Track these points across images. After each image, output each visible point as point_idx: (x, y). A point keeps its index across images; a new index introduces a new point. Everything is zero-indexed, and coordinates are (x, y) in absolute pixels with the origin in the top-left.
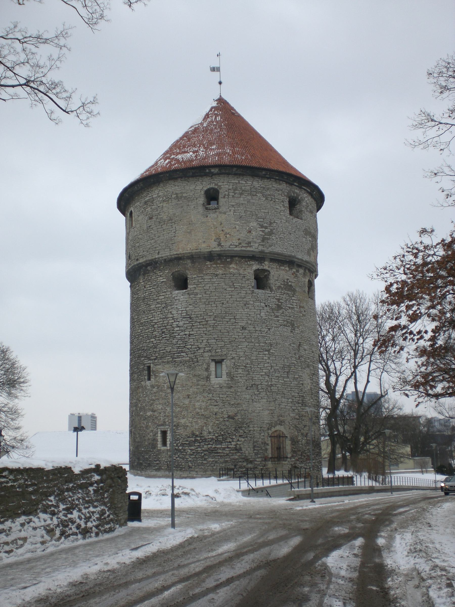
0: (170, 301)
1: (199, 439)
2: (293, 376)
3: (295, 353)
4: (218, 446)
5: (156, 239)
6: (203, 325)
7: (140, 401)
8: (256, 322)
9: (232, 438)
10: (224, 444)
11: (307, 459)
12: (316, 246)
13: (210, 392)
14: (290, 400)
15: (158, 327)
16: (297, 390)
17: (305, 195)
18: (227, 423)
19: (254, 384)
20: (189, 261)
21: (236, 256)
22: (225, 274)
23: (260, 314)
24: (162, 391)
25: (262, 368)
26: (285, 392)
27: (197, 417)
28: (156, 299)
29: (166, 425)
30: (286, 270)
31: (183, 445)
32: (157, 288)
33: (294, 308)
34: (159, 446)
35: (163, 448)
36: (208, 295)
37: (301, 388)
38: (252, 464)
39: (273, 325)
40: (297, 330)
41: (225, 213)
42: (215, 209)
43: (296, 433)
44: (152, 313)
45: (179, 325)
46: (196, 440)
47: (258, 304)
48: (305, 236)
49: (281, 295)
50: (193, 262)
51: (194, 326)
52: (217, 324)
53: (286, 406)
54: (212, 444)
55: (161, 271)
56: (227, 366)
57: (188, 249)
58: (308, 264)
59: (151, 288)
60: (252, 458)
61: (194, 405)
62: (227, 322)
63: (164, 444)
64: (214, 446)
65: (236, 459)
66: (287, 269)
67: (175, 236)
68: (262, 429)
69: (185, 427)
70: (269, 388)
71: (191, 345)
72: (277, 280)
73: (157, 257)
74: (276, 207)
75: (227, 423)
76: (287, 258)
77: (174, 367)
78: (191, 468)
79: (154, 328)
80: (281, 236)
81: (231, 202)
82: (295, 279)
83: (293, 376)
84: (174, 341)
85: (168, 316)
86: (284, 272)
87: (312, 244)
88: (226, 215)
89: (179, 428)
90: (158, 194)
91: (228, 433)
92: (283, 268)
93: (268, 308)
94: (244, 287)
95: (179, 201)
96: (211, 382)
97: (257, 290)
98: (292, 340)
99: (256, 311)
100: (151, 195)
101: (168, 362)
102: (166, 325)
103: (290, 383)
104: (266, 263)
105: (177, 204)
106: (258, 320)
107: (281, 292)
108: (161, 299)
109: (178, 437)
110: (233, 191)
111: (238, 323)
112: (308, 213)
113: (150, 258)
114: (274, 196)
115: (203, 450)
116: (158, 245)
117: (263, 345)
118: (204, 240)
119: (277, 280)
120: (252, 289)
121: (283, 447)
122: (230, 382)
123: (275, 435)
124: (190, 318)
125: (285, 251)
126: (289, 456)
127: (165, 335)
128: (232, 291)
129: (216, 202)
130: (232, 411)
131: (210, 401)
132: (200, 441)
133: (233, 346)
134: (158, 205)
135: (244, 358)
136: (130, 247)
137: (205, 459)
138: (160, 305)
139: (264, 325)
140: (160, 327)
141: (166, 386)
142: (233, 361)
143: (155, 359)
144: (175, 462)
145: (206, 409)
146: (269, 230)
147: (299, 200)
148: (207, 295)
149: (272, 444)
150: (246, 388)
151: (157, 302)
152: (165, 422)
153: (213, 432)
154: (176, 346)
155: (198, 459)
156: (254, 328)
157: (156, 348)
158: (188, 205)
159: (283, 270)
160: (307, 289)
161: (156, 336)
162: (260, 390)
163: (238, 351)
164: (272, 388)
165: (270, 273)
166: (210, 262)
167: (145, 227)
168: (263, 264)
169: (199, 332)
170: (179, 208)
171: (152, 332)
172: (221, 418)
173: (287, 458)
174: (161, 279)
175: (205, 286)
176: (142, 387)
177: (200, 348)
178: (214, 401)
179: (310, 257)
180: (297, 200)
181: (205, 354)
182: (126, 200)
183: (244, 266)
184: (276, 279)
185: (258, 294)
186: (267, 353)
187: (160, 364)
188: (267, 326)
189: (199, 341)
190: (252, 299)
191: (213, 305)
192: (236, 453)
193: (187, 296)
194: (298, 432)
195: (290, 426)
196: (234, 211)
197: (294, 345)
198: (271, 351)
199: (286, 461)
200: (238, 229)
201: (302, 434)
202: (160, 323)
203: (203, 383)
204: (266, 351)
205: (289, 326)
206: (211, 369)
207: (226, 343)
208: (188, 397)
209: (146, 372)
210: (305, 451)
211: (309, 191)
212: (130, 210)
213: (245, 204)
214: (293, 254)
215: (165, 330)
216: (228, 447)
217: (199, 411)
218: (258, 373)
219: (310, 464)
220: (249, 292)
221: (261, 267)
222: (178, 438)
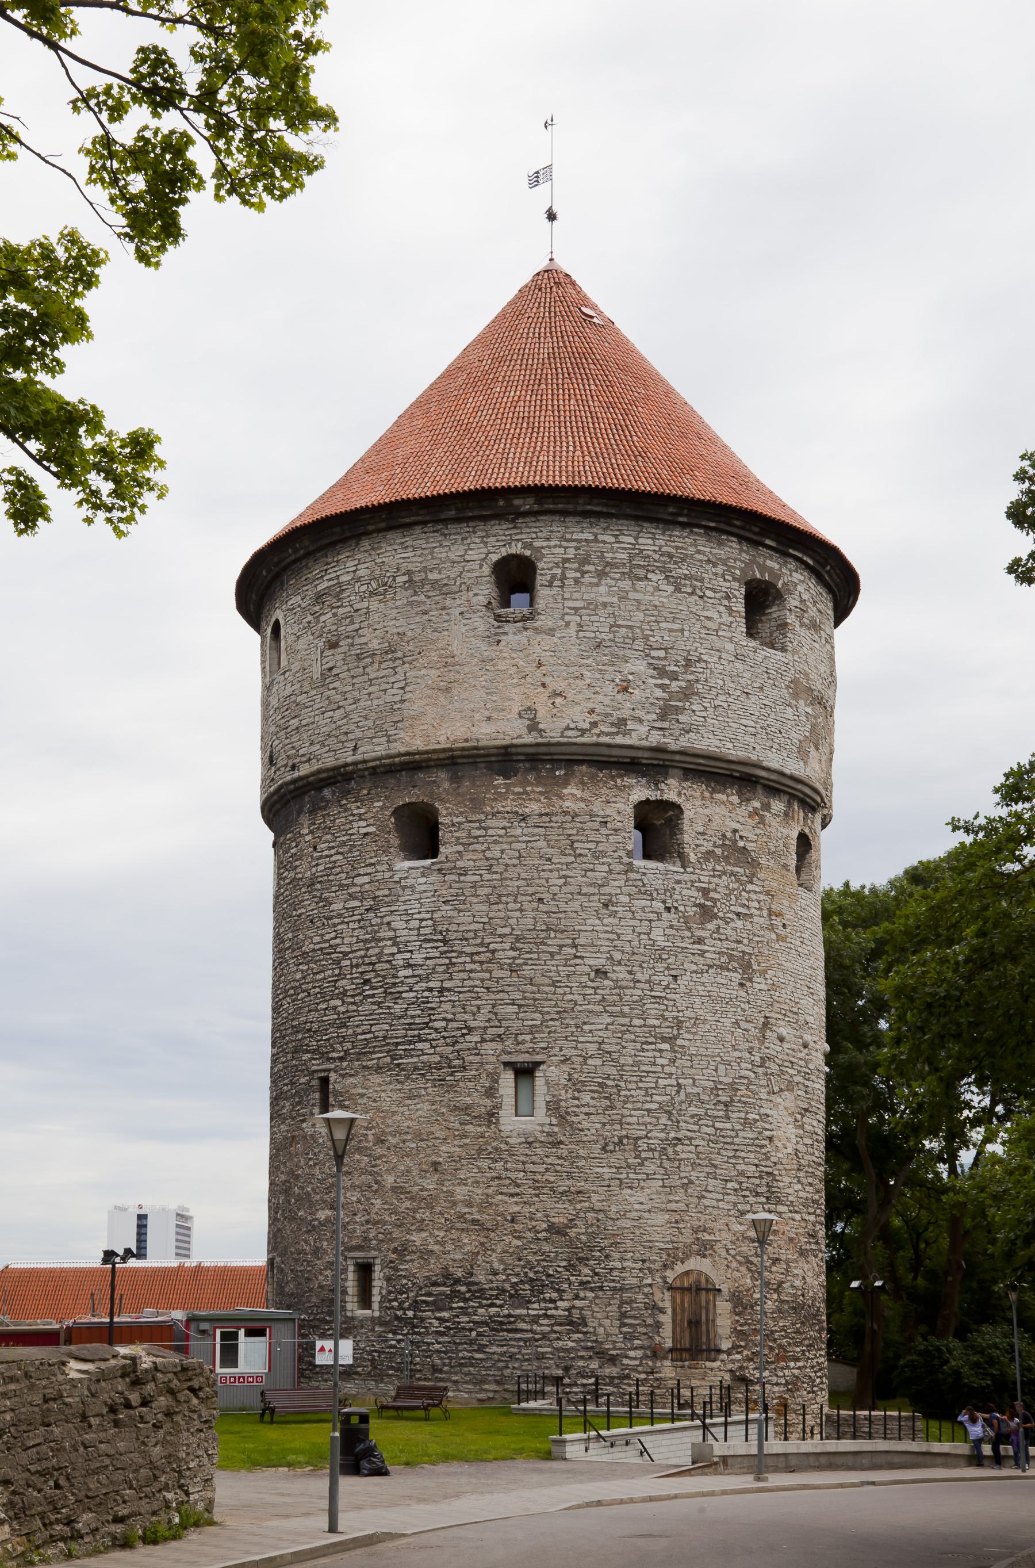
0: (387, 892)
1: (463, 1289)
2: (742, 1115)
3: (752, 1048)
4: (518, 1312)
5: (349, 708)
6: (481, 963)
7: (297, 1177)
8: (635, 957)
9: (558, 1291)
10: (536, 1306)
11: (778, 1358)
12: (830, 730)
13: (496, 1155)
14: (730, 1185)
16: (752, 1156)
17: (797, 576)
18: (546, 1247)
19: (626, 1137)
20: (443, 775)
21: (581, 762)
22: (547, 814)
23: (648, 934)
25: (650, 1091)
26: (718, 1160)
27: (459, 1225)
28: (348, 886)
29: (370, 1249)
30: (732, 804)
31: (416, 1305)
32: (350, 851)
33: (752, 915)
34: (349, 1306)
35: (361, 1313)
36: (497, 877)
37: (764, 1150)
38: (615, 1365)
39: (687, 966)
40: (759, 983)
41: (551, 632)
42: (524, 619)
43: (749, 1281)
44: (335, 925)
45: (411, 962)
46: (455, 1294)
47: (643, 903)
48: (793, 702)
49: (714, 876)
50: (455, 779)
51: (454, 964)
52: (521, 961)
53: (718, 1201)
54: (501, 1306)
55: (362, 801)
56: (547, 1083)
57: (442, 739)
59: (333, 852)
60: (614, 1349)
61: (451, 1193)
62: (552, 954)
63: (365, 1301)
64: (506, 1312)
65: (567, 1350)
66: (735, 799)
67: (402, 701)
68: (647, 1265)
69: (426, 1254)
70: (670, 1150)
71: (444, 1019)
72: (704, 834)
73: (349, 760)
74: (706, 613)
75: (546, 1247)
76: (733, 767)
78: (441, 1371)
79: (341, 968)
80: (717, 703)
81: (568, 599)
82: (758, 831)
83: (742, 1115)
84: (397, 1009)
86: (725, 811)
87: (813, 725)
88: (556, 640)
89: (408, 1258)
90: (354, 571)
91: (549, 1276)
93: (672, 916)
94: (604, 854)
95: (416, 593)
96: (502, 1128)
97: (639, 863)
99: (637, 923)
100: (333, 575)
101: (378, 1069)
103: (733, 1134)
104: (670, 781)
105: (411, 604)
106: (642, 950)
107: (714, 870)
108: (361, 886)
109: (404, 1281)
110: (577, 565)
111: (582, 958)
112: (803, 631)
113: (329, 762)
114: (702, 581)
115: (475, 1323)
116: (353, 727)
117: (656, 1022)
118: (487, 713)
119: (704, 834)
120: (626, 860)
121: (707, 1320)
122: (556, 1129)
123: (686, 1285)
124: (445, 942)
125: (730, 746)
126: (725, 1345)
127: (372, 988)
128: (567, 864)
129: (527, 596)
130: (560, 1212)
131: (497, 1182)
132: (468, 1295)
133: (568, 1026)
134: (356, 607)
135: (599, 1062)
136: (273, 729)
137: (481, 1349)
138: (357, 903)
139: (660, 966)
140: (357, 966)
141: (371, 1138)
142: (566, 1068)
144: (395, 1354)
145: (486, 1204)
146: (683, 684)
147: (778, 591)
148: (495, 876)
149: (674, 1310)
150: (604, 1149)
151: (350, 895)
152: (366, 1239)
153: (505, 1270)
154: (402, 1021)
155: (460, 1347)
156: (630, 973)
157: (344, 1025)
158: (444, 608)
159: (723, 803)
160: (792, 860)
161: (346, 991)
162: (643, 1155)
163: (581, 1039)
164: (679, 1148)
165: (682, 812)
166: (507, 777)
168: (663, 786)
169: (471, 983)
170: (417, 613)
171: (336, 981)
172: (530, 1230)
173: (719, 1351)
174: (361, 827)
175: (489, 849)
176: (305, 1137)
177: (470, 1030)
178: (508, 1182)
179: (806, 763)
180: (773, 591)
181: (485, 1046)
182: (260, 587)
183: (604, 791)
184: (701, 830)
185: (644, 874)
186: (666, 1046)
188: (668, 968)
189: (468, 1008)
190: (625, 890)
191: (511, 906)
192: (569, 1332)
193: (434, 878)
194: (753, 1278)
195: (730, 1258)
196: (580, 625)
197: (749, 1026)
198: (679, 1042)
199: (714, 1361)
200: (588, 681)
201: (767, 1284)
202: (358, 954)
203: (479, 1129)
204: (664, 1039)
205: (734, 970)
206: (501, 1092)
207: (547, 1017)
208: (436, 1170)
209: (317, 1095)
210: (773, 1332)
211: (811, 562)
212: (273, 620)
213: (612, 604)
214: (754, 757)
216: (546, 1316)
217: (467, 1210)
218: (639, 1105)
219: (786, 1372)
220: (619, 868)
221: (653, 795)
222: (403, 1286)
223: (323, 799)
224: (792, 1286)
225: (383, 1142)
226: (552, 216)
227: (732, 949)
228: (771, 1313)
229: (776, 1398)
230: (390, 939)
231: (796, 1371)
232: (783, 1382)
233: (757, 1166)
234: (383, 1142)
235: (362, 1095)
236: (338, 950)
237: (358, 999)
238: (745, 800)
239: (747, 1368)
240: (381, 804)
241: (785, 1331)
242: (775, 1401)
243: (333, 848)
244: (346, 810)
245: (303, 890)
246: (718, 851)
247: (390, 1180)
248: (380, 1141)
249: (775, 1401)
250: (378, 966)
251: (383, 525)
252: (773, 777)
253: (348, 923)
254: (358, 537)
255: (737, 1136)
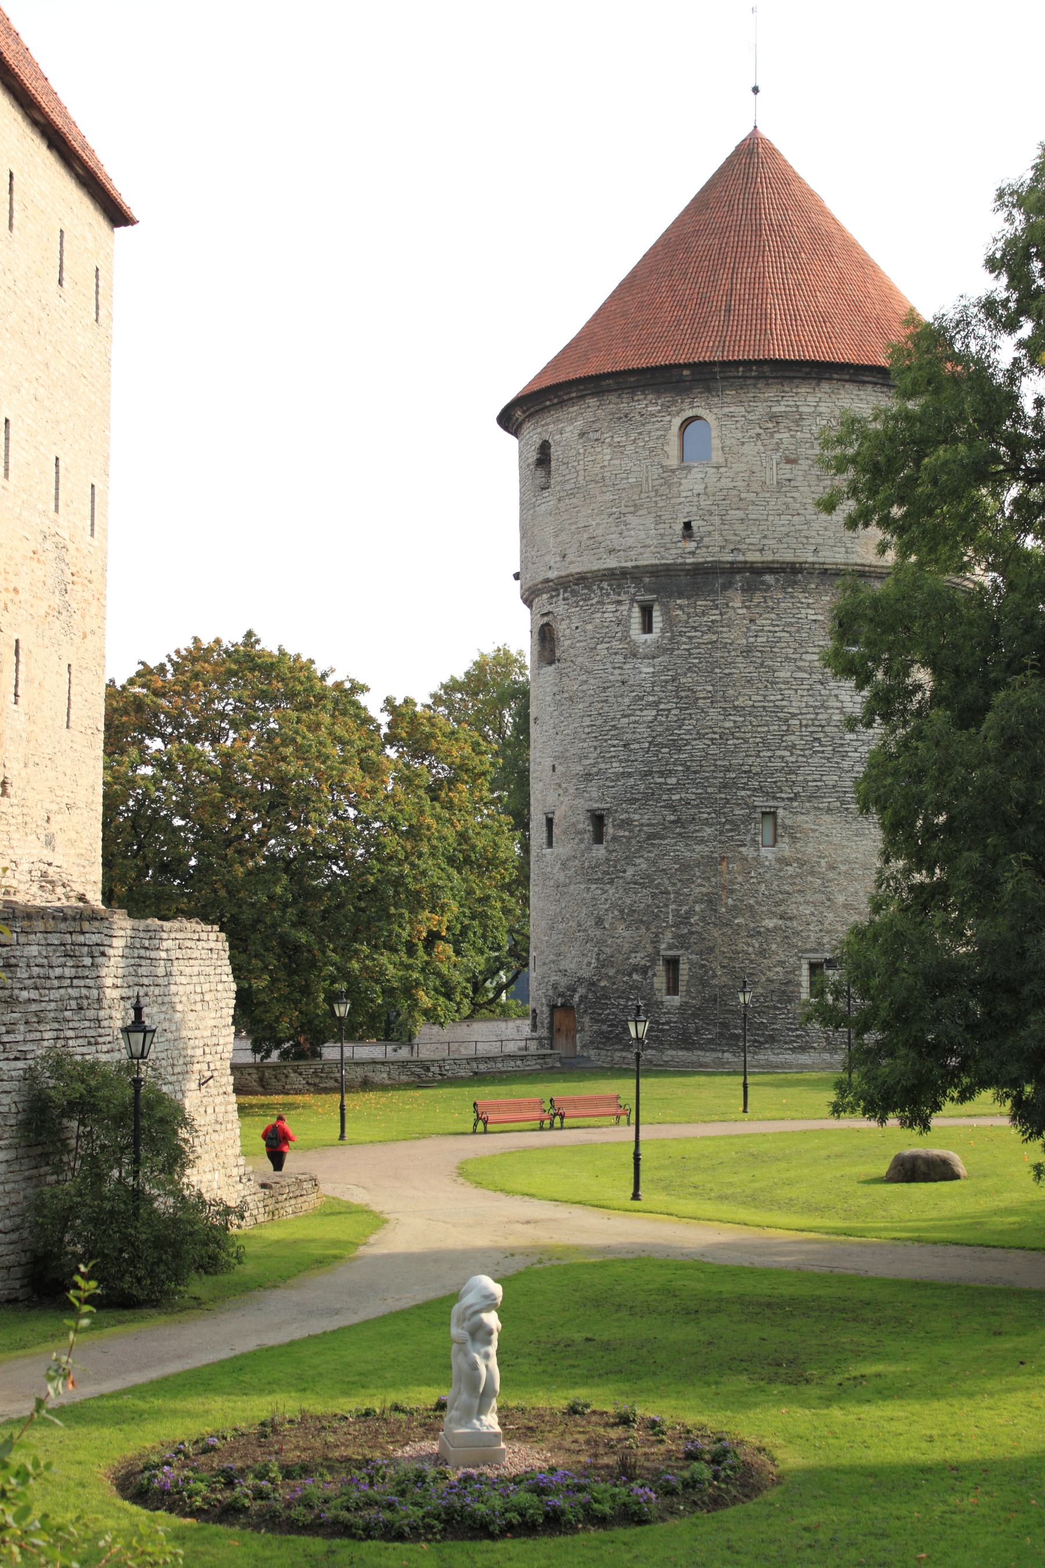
15: (801, 725)
24: (812, 873)
28: (795, 660)
29: (824, 951)
32: (798, 631)
44: (781, 690)
59: (777, 629)
73: (810, 560)
77: (844, 823)
79: (789, 725)
84: (845, 764)
85: (830, 704)
101: (829, 811)
102: (823, 723)
108: (810, 662)
113: (789, 557)
116: (814, 533)
127: (821, 745)
140: (806, 726)
143: (790, 799)
151: (798, 667)
154: (849, 774)
167: (772, 477)
187: (808, 813)
202: (808, 716)
215: (822, 735)
223: (763, 583)
225: (834, 868)
226: (756, 90)
230: (838, 708)
234: (834, 868)
235: (814, 831)
236: (786, 710)
237: (807, 752)
240: (828, 598)
243: (778, 625)
244: (792, 597)
245: (733, 653)
247: (841, 899)
248: (832, 867)
250: (827, 729)
251: (847, 377)
253: (796, 690)
254: (819, 379)
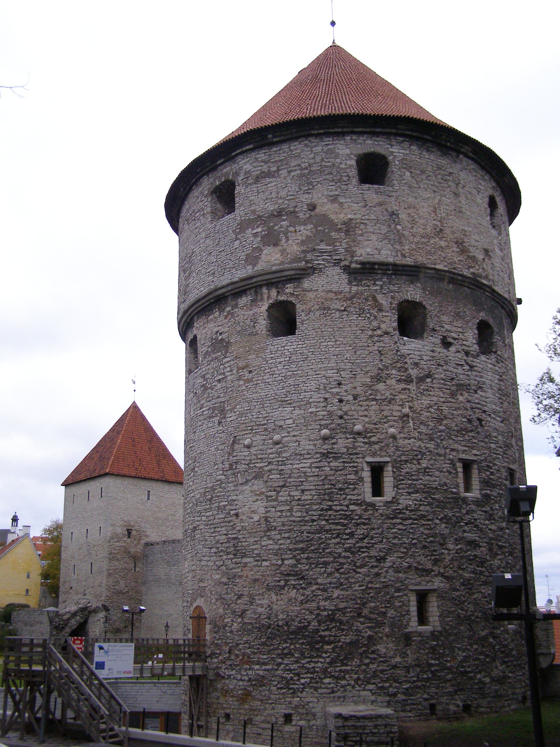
11: (243, 662)
16: (223, 529)
37: (231, 524)
58: (254, 280)
76: (207, 298)
92: (212, 317)
98: (221, 438)
103: (212, 518)
159: (212, 320)
194: (224, 609)
198: (196, 469)
201: (234, 612)
211: (251, 146)
219: (250, 672)
224: (255, 613)
227: (216, 403)
228: (237, 631)
229: (241, 690)
231: (261, 673)
232: (247, 678)
233: (226, 535)
238: (222, 310)
239: (221, 668)
241: (250, 644)
242: (240, 692)
246: (210, 350)
249: (240, 692)
252: (229, 288)
255: (215, 519)
